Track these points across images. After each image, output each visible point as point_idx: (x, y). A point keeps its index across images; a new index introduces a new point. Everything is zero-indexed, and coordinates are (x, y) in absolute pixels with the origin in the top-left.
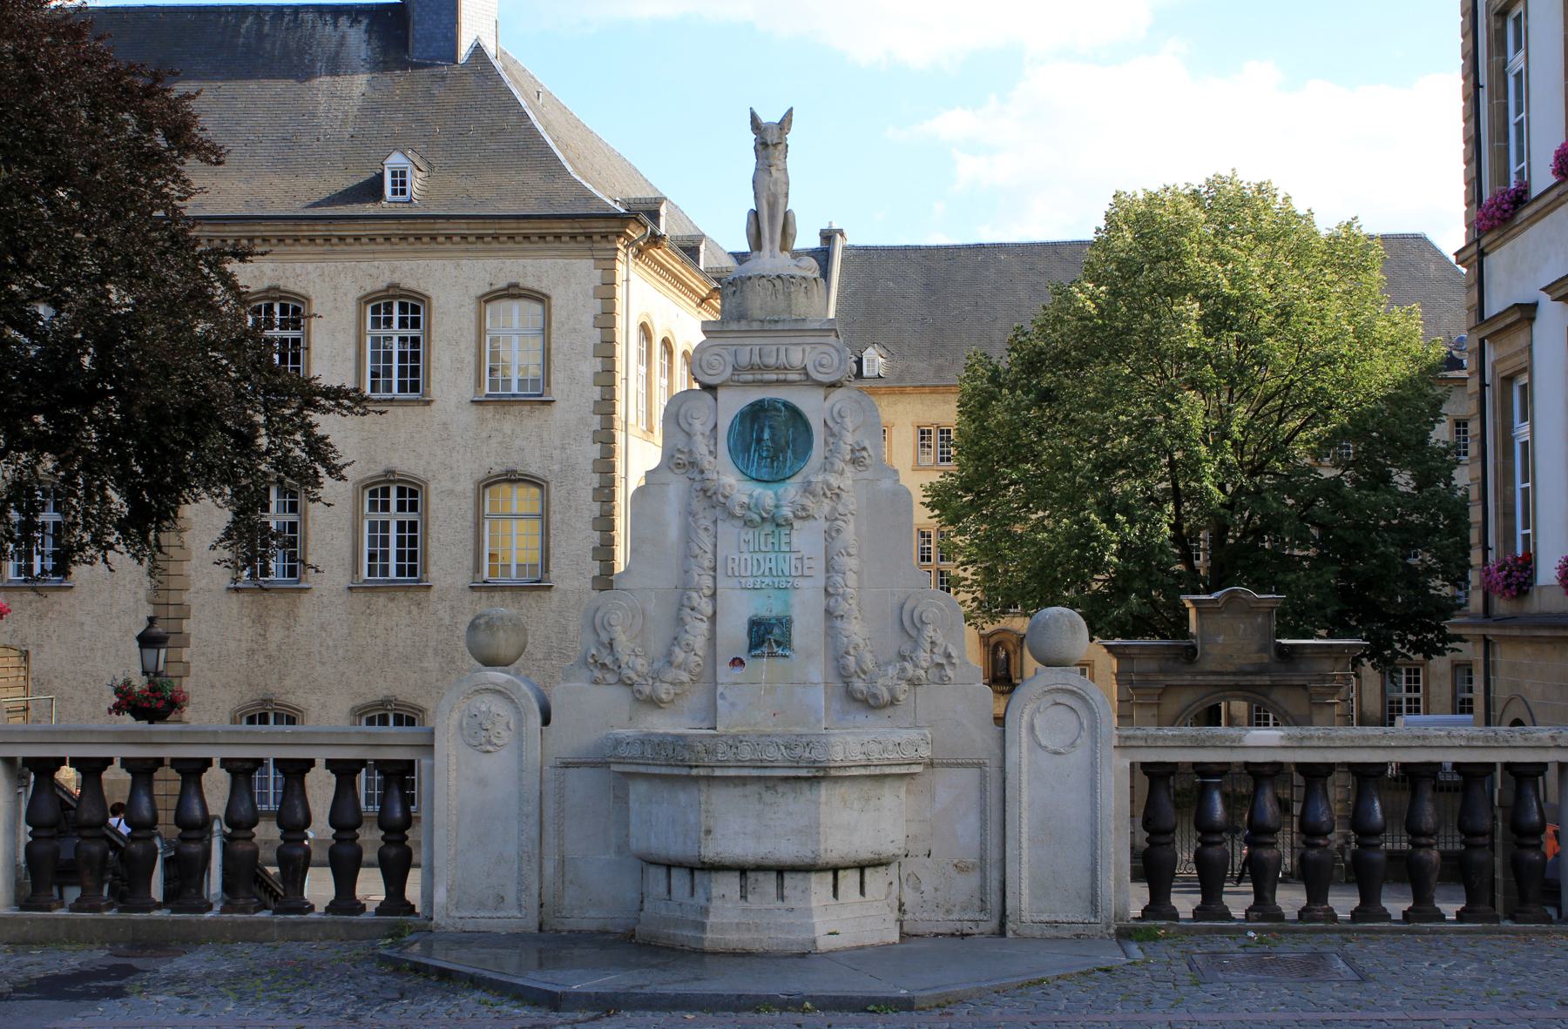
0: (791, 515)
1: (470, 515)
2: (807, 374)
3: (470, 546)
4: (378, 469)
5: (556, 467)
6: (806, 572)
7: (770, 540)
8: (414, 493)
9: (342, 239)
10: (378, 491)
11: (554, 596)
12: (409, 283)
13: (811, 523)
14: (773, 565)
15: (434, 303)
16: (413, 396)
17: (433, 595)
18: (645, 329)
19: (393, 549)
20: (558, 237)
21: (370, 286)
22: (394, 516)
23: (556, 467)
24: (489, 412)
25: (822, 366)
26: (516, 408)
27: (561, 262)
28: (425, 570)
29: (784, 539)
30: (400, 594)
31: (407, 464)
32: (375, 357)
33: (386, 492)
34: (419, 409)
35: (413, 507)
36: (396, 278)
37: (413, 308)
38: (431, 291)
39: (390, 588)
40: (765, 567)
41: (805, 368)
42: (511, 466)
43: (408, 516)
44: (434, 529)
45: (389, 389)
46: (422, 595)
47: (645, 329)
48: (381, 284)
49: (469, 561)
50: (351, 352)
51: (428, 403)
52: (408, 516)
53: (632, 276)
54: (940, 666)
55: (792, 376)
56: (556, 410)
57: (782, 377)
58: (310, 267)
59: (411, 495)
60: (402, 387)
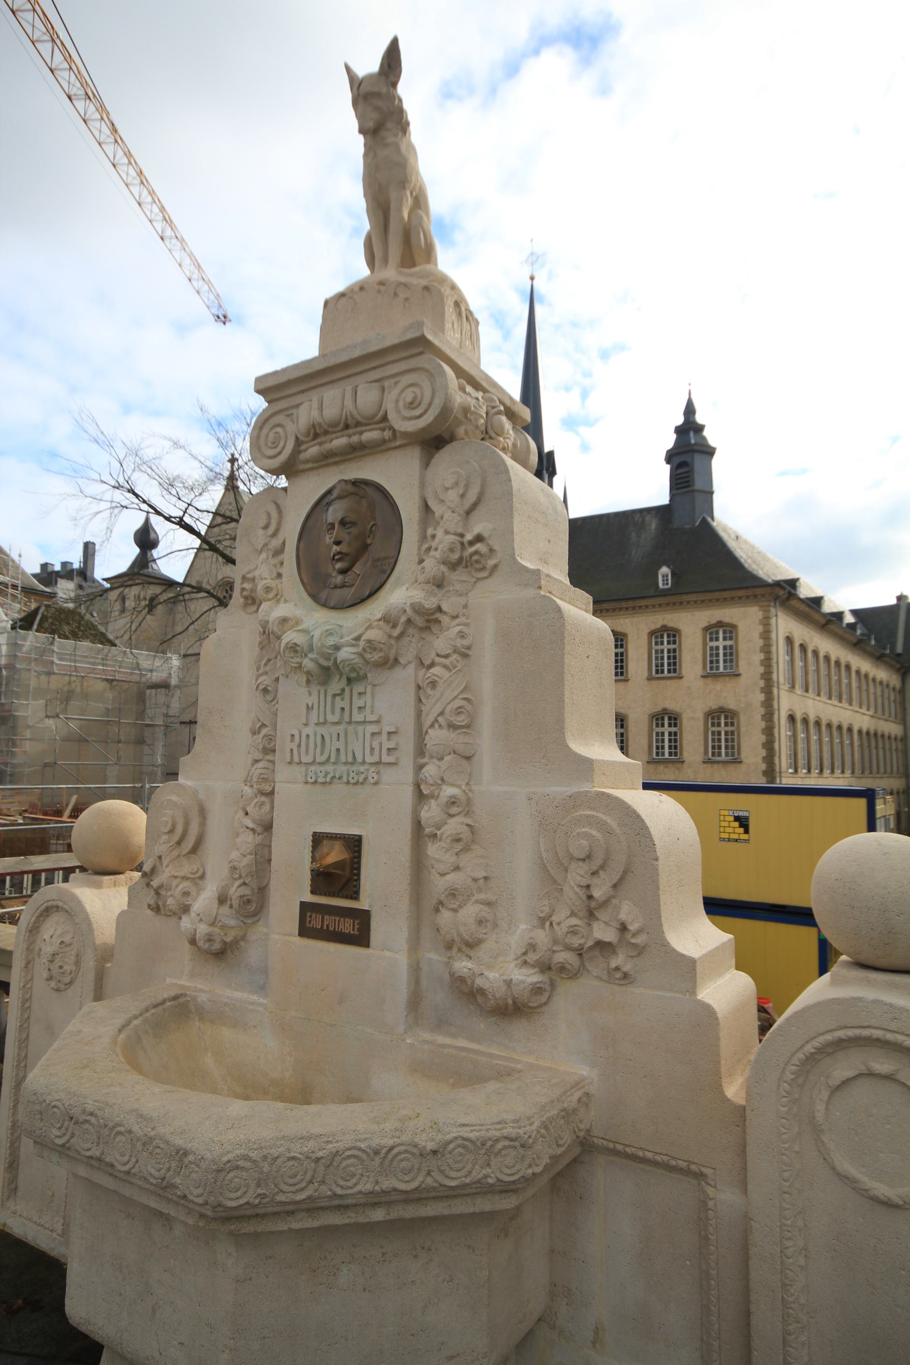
0: (357, 660)
1: (702, 729)
2: (391, 428)
3: (702, 743)
4: (659, 709)
5: (742, 705)
6: (386, 759)
7: (339, 703)
8: (675, 719)
9: (640, 607)
10: (658, 718)
11: (743, 767)
12: (671, 624)
13: (399, 674)
14: (341, 745)
15: (683, 633)
16: (672, 675)
17: (685, 765)
18: (789, 640)
19: (666, 744)
20: (740, 598)
21: (653, 627)
22: (666, 729)
23: (742, 705)
24: (709, 681)
25: (412, 405)
26: (722, 679)
27: (742, 609)
28: (681, 754)
29: (358, 703)
30: (670, 765)
31: (671, 706)
32: (657, 658)
33: (663, 719)
34: (676, 681)
35: (675, 725)
36: (665, 623)
37: (673, 634)
38: (681, 628)
39: (666, 762)
40: (333, 745)
41: (385, 419)
42: (720, 705)
43: (673, 729)
44: (685, 735)
45: (662, 672)
46: (680, 765)
47: (789, 640)
48: (658, 626)
49: (702, 749)
50: (646, 656)
51: (681, 678)
52: (673, 729)
53: (779, 613)
54: (601, 945)
55: (371, 435)
56: (742, 679)
57: (355, 439)
58: (627, 621)
59: (675, 719)
60: (669, 671)
